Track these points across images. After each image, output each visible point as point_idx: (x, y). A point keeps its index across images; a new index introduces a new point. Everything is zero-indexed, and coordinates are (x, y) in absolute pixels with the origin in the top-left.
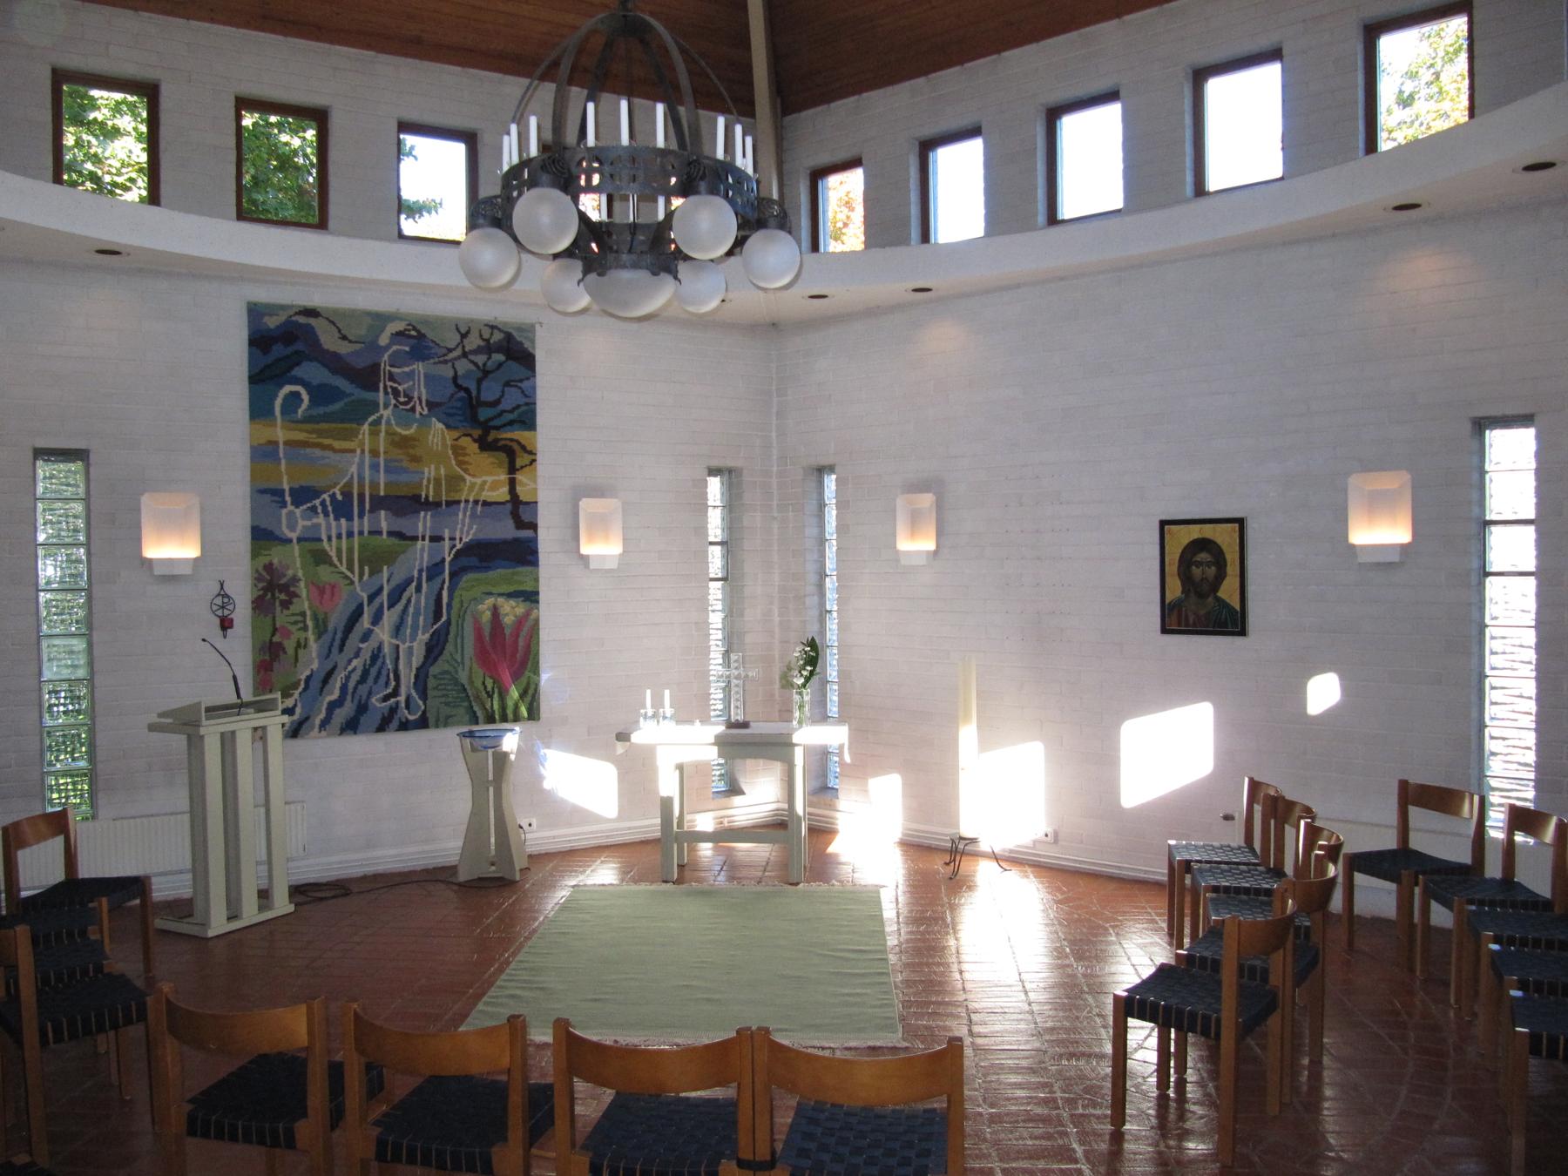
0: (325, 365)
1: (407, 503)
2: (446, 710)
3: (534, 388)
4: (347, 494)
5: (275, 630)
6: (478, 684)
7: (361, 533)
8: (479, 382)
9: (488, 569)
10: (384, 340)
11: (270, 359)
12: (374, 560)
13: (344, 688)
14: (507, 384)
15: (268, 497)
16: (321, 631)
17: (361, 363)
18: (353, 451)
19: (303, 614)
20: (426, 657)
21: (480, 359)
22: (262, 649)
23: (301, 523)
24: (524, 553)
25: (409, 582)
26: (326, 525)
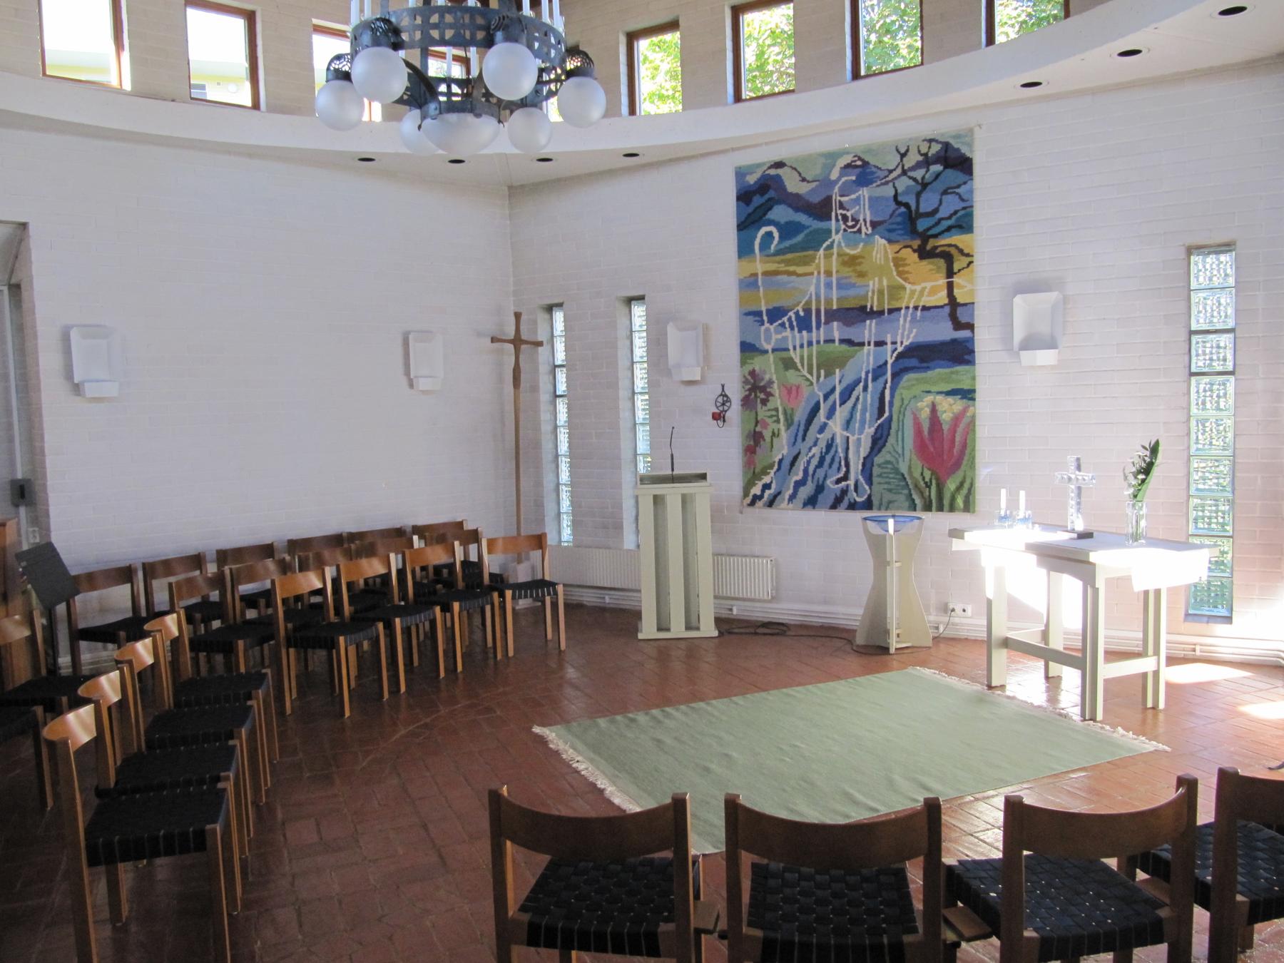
0: (790, 206)
1: (857, 314)
2: (888, 497)
3: (971, 192)
4: (808, 311)
5: (757, 422)
6: (917, 474)
7: (818, 342)
8: (918, 195)
9: (928, 368)
10: (834, 175)
11: (750, 209)
12: (828, 365)
13: (806, 471)
14: (945, 192)
15: (751, 318)
16: (789, 423)
17: (816, 199)
18: (812, 274)
19: (776, 410)
20: (872, 449)
21: (919, 174)
22: (748, 437)
23: (775, 337)
24: (959, 353)
25: (858, 382)
26: (793, 337)
